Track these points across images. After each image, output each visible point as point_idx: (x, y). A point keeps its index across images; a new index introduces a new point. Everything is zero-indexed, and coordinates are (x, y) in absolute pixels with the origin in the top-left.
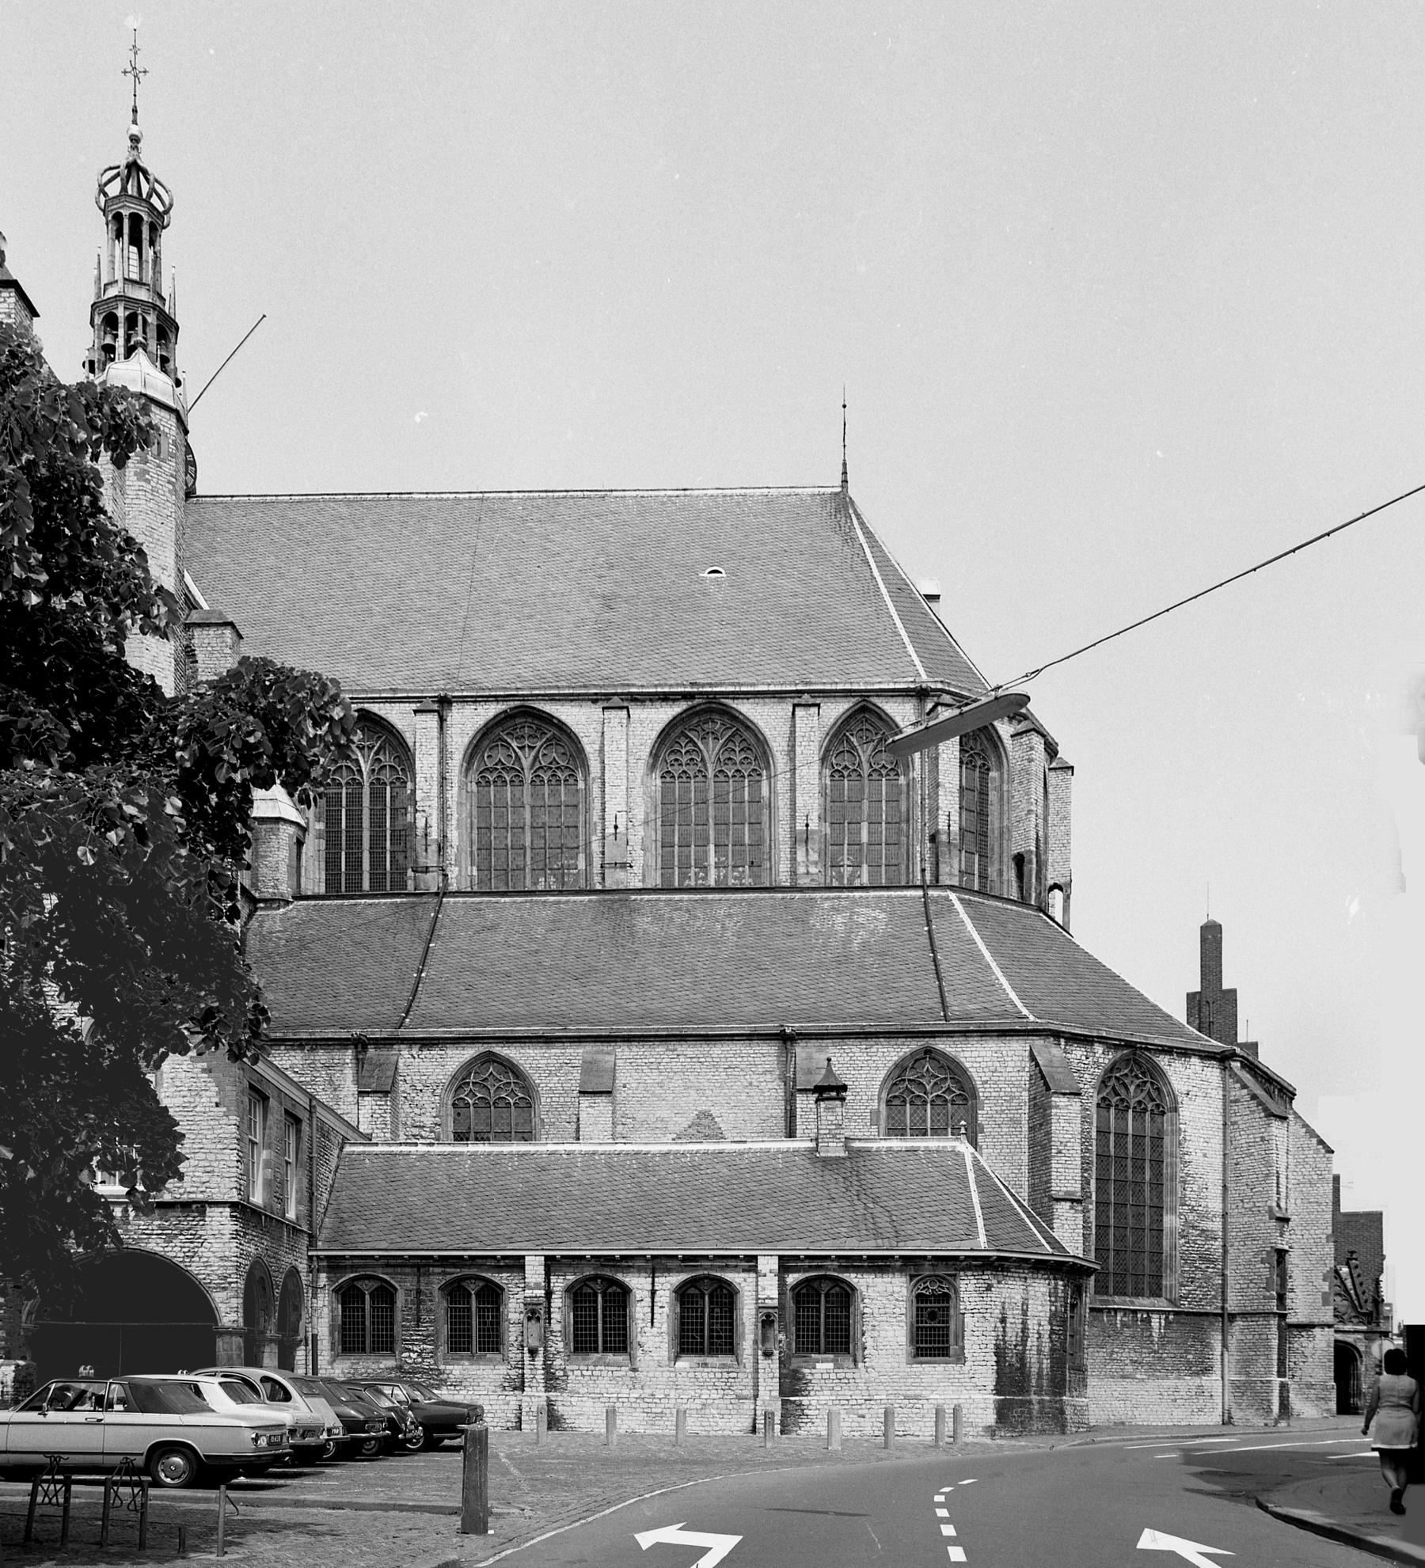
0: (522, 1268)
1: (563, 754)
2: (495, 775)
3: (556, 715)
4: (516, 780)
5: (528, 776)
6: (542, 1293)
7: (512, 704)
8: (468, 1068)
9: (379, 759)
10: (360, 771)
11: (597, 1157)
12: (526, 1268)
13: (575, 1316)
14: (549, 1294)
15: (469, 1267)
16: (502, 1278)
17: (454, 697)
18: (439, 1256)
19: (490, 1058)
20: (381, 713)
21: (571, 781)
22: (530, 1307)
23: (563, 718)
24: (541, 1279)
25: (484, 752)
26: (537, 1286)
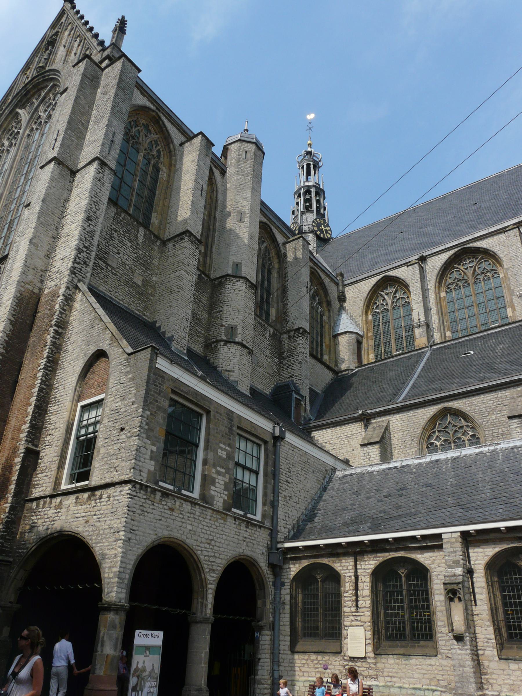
0: (440, 547)
1: (489, 264)
2: (454, 285)
3: (480, 246)
4: (466, 284)
5: (471, 280)
6: (459, 571)
7: (457, 249)
8: (434, 420)
9: (396, 297)
10: (387, 304)
11: (516, 450)
12: (444, 546)
13: (504, 597)
14: (470, 572)
15: (396, 550)
16: (424, 558)
17: (427, 256)
18: (371, 541)
19: (446, 411)
20: (394, 275)
21: (496, 275)
22: (450, 587)
23: (485, 246)
24: (459, 557)
25: (447, 276)
26: (456, 563)
